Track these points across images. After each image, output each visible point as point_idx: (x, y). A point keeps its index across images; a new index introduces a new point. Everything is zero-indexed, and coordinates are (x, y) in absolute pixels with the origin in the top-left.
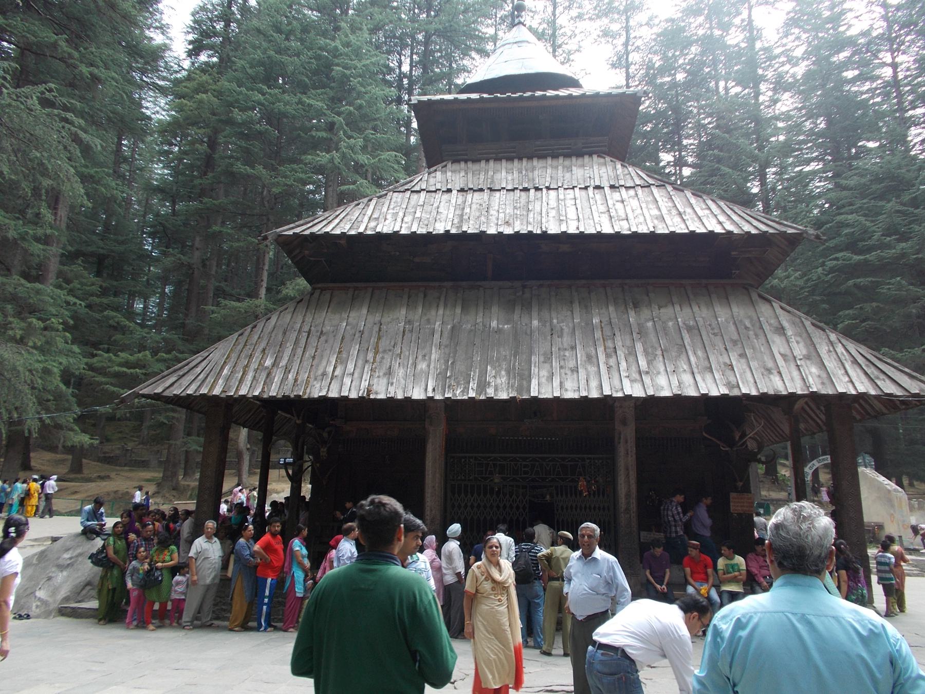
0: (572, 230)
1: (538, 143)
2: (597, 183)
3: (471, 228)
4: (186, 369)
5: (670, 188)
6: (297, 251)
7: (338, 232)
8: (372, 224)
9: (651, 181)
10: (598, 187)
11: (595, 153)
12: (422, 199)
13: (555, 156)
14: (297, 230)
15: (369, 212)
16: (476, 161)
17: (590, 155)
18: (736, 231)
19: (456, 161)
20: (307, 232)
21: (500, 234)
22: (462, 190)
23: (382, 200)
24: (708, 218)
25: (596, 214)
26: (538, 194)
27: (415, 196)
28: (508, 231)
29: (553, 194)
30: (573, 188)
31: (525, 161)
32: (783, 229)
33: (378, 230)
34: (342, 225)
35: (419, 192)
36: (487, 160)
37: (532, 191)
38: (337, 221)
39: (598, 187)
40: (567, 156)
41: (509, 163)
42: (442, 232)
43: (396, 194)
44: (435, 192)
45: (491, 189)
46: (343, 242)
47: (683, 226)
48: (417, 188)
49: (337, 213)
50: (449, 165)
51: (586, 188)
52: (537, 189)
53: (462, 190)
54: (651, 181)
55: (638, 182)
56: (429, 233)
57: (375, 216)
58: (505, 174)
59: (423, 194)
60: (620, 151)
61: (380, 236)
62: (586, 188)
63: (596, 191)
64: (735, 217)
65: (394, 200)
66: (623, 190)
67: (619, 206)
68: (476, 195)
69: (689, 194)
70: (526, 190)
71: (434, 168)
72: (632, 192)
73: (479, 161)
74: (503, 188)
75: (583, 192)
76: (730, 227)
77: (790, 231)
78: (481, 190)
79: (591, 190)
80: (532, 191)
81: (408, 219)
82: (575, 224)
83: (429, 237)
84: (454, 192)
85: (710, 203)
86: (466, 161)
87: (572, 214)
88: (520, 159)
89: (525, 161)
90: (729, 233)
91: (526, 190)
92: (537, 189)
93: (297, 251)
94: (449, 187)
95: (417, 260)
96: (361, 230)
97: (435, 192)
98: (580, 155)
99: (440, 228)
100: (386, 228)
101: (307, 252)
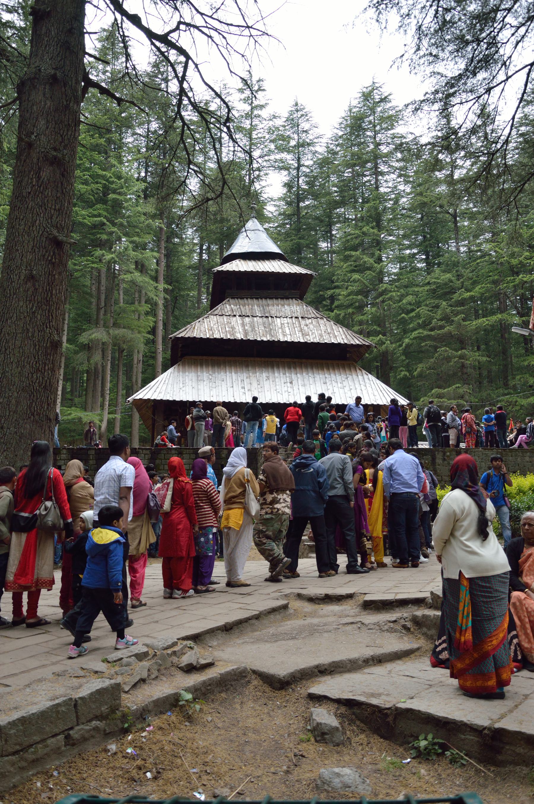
3: (251, 337)
5: (325, 320)
8: (211, 332)
9: (318, 316)
10: (296, 318)
13: (277, 298)
14: (182, 335)
16: (242, 298)
17: (292, 298)
19: (233, 298)
21: (262, 340)
22: (240, 316)
24: (339, 336)
25: (297, 332)
28: (265, 339)
29: (278, 319)
35: (223, 315)
39: (296, 318)
40: (282, 298)
48: (220, 314)
52: (272, 317)
54: (318, 316)
55: (313, 316)
58: (255, 307)
64: (348, 336)
67: (306, 328)
68: (247, 318)
69: (332, 323)
70: (267, 317)
72: (310, 321)
73: (243, 298)
75: (291, 320)
76: (346, 342)
77: (367, 344)
78: (248, 316)
82: (289, 337)
85: (340, 329)
86: (237, 298)
90: (346, 344)
91: (267, 317)
92: (272, 317)
94: (235, 313)
98: (287, 298)
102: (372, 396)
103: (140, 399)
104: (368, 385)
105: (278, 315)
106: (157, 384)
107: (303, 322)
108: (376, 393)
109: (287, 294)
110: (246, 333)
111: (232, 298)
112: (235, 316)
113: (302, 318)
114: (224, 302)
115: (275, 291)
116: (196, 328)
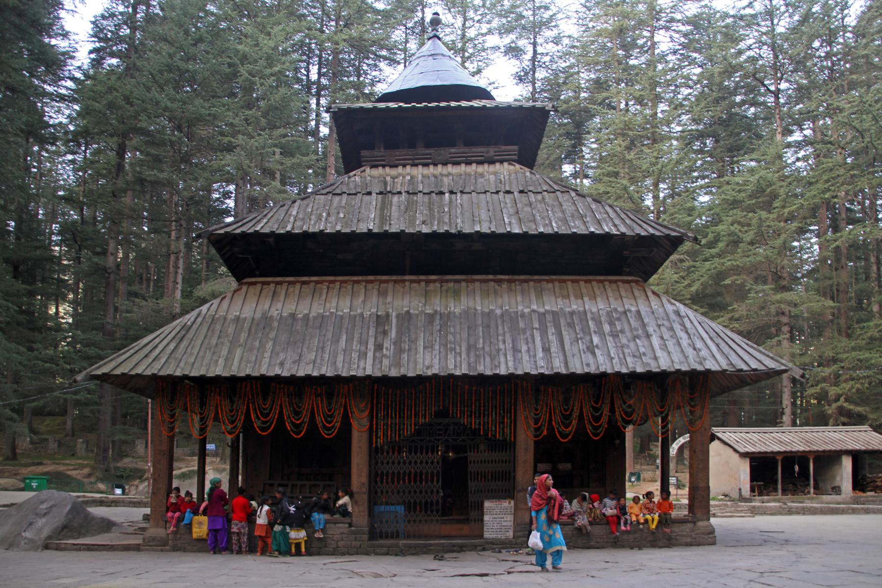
0: (485, 229)
1: (453, 150)
2: (508, 189)
4: (132, 351)
6: (227, 249)
7: (266, 230)
9: (556, 187)
10: (508, 192)
11: (506, 161)
12: (344, 202)
15: (294, 213)
17: (501, 162)
18: (629, 233)
20: (238, 231)
22: (381, 193)
23: (305, 202)
26: (454, 196)
27: (337, 198)
29: (465, 196)
30: (485, 192)
31: (440, 166)
32: (667, 232)
33: (305, 228)
34: (270, 224)
36: (404, 166)
37: (447, 195)
38: (265, 221)
39: (508, 192)
41: (426, 168)
42: (365, 231)
43: (317, 197)
44: (355, 194)
45: (408, 192)
46: (271, 240)
47: (583, 227)
49: (265, 212)
50: (368, 170)
51: (497, 192)
52: (451, 192)
53: (381, 193)
54: (556, 187)
56: (353, 232)
57: (301, 216)
59: (345, 196)
60: (528, 160)
61: (306, 235)
62: (497, 192)
63: (507, 195)
65: (316, 202)
66: (531, 195)
71: (354, 173)
72: (539, 197)
74: (420, 192)
79: (501, 194)
80: (447, 195)
81: (332, 219)
83: (353, 237)
84: (374, 195)
86: (384, 166)
87: (484, 215)
88: (435, 165)
89: (440, 166)
93: (227, 249)
95: (340, 256)
96: (289, 228)
97: (355, 194)
99: (362, 228)
100: (314, 227)
101: (236, 249)
102: (690, 352)
103: (123, 374)
104: (677, 327)
105: (467, 190)
106: (157, 340)
107: (521, 199)
108: (699, 344)
109: (492, 153)
110: (384, 218)
111: (372, 167)
112: (369, 193)
113: (521, 192)
114: (351, 174)
115: (466, 150)
116: (269, 216)
